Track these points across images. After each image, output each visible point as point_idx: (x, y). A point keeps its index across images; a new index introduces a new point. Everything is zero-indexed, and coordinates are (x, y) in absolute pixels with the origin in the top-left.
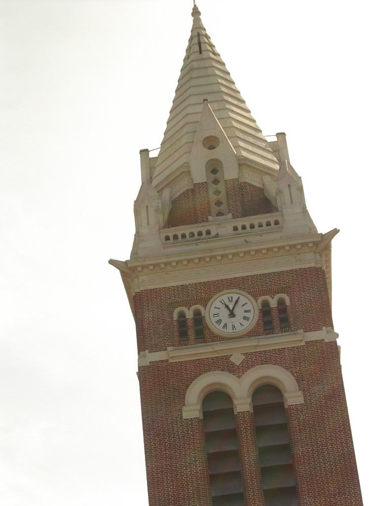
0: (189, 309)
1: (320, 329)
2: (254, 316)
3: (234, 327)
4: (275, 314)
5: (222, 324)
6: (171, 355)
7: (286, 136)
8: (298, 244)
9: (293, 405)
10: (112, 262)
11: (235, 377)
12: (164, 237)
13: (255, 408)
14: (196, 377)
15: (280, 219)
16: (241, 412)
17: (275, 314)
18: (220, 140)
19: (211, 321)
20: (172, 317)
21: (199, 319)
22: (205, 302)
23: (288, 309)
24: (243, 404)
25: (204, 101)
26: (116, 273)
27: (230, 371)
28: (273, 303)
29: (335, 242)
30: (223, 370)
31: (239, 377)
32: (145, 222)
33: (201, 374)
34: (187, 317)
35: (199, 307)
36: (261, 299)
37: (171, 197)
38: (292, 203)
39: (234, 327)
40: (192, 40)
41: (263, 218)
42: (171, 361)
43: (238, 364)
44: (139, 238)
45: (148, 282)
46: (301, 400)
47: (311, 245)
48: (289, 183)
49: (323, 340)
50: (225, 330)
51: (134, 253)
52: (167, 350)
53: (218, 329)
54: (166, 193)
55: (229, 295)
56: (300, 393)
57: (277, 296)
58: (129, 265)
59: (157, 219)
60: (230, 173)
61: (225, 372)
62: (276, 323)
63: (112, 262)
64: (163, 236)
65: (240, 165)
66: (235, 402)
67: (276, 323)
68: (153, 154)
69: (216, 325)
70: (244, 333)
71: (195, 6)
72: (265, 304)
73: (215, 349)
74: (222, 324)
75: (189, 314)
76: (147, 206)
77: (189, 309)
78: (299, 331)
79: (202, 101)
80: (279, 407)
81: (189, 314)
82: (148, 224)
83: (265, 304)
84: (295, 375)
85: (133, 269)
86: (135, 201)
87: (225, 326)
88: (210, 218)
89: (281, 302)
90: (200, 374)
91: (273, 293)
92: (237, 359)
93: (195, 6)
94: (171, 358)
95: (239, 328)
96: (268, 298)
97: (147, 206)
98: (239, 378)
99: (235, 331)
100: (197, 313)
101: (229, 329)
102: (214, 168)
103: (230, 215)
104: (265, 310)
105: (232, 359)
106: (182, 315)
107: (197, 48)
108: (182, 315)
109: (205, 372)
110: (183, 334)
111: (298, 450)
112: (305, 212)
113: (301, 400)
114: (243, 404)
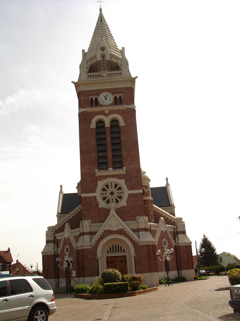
1: (131, 105)
2: (112, 100)
3: (106, 103)
4: (118, 100)
5: (103, 102)
10: (72, 82)
15: (121, 72)
17: (118, 100)
19: (100, 101)
20: (89, 99)
21: (96, 100)
23: (122, 98)
24: (107, 125)
26: (74, 85)
28: (118, 96)
29: (136, 80)
36: (114, 95)
39: (106, 103)
41: (117, 72)
42: (88, 111)
45: (82, 88)
46: (124, 125)
51: (79, 80)
53: (102, 103)
54: (89, 62)
55: (106, 93)
56: (124, 122)
57: (119, 95)
59: (86, 70)
62: (118, 102)
63: (72, 82)
67: (118, 102)
68: (86, 51)
72: (116, 97)
74: (103, 102)
75: (94, 98)
80: (118, 126)
81: (94, 98)
83: (116, 97)
85: (78, 84)
86: (80, 65)
87: (104, 102)
88: (101, 71)
89: (120, 96)
91: (118, 93)
92: (107, 112)
95: (108, 103)
96: (116, 95)
100: (96, 98)
101: (105, 103)
102: (103, 56)
103: (107, 70)
104: (115, 98)
105: (105, 112)
106: (92, 98)
107: (100, 21)
111: (122, 138)
113: (124, 125)
114: (107, 125)
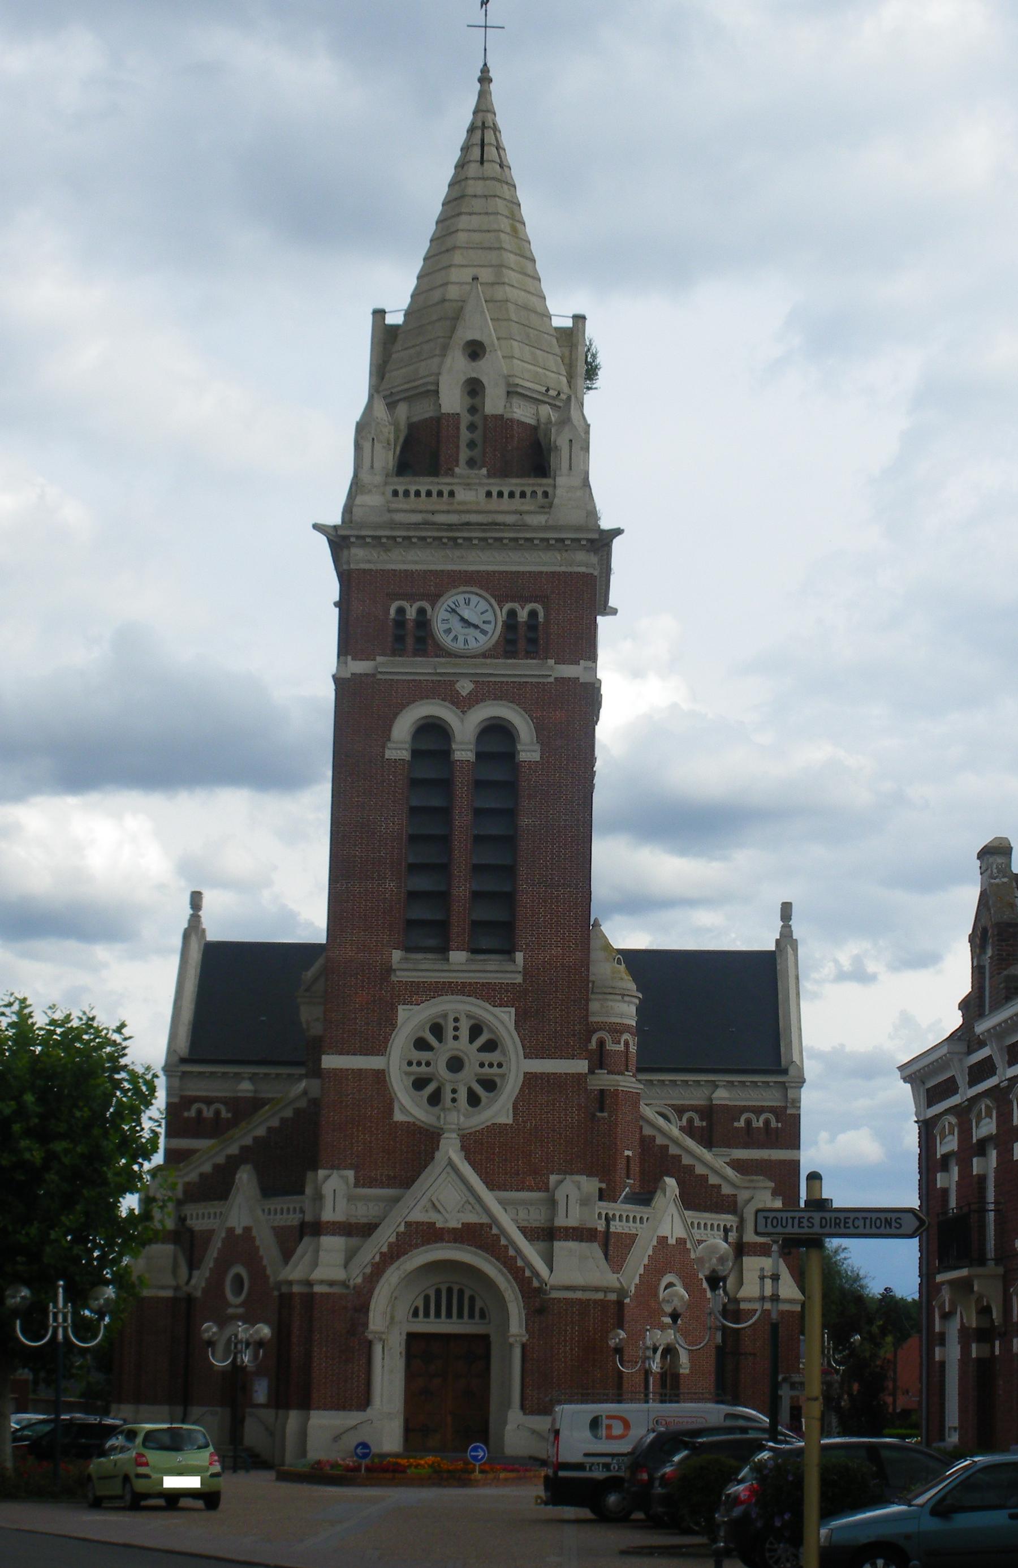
0: (411, 606)
1: (577, 663)
2: (495, 631)
3: (466, 641)
4: (522, 631)
5: (452, 636)
6: (379, 670)
7: (587, 321)
8: (568, 539)
9: (526, 761)
10: (316, 527)
11: (458, 711)
12: (391, 491)
13: (479, 755)
14: (408, 704)
15: (550, 490)
16: (459, 761)
17: (522, 631)
18: (488, 350)
19: (439, 627)
20: (387, 612)
21: (423, 622)
22: (434, 598)
23: (540, 628)
24: (464, 751)
25: (473, 279)
26: (322, 543)
27: (453, 703)
28: (523, 615)
29: (617, 543)
30: (444, 700)
31: (464, 712)
32: (367, 463)
33: (415, 701)
34: (407, 617)
35: (425, 604)
36: (508, 606)
37: (408, 418)
38: (570, 469)
39: (466, 641)
40: (472, 131)
41: (528, 484)
42: (379, 676)
43: (464, 695)
44: (356, 487)
45: (360, 557)
46: (536, 756)
47: (584, 542)
48: (571, 438)
49: (578, 678)
50: (454, 645)
51: (348, 509)
52: (375, 660)
53: (446, 640)
54: (402, 409)
55: (467, 596)
56: (537, 747)
57: (529, 607)
58: (341, 532)
59: (386, 458)
60: (494, 403)
61: (446, 703)
62: (522, 644)
63: (316, 527)
64: (389, 490)
65: (508, 393)
66: (453, 746)
67: (522, 644)
68: (396, 319)
69: (444, 636)
70: (478, 653)
71: (485, 65)
72: (512, 614)
73: (438, 671)
74: (452, 636)
75: (411, 613)
76: (373, 439)
77: (411, 606)
78: (549, 660)
79: (471, 281)
80: (509, 756)
81: (411, 613)
82: (372, 467)
83: (512, 614)
84: (535, 721)
85: (345, 538)
86: (358, 424)
87: (456, 638)
88: (457, 470)
89: (533, 614)
90: (414, 701)
91: (524, 600)
92: (465, 687)
93: (485, 65)
94: (380, 673)
95: (472, 644)
96: (516, 606)
97: (373, 439)
98: (463, 714)
99: (467, 647)
100: (422, 611)
101: (460, 644)
102: (474, 388)
103: (484, 471)
104: (511, 623)
105: (458, 686)
106: (401, 611)
107: (476, 152)
108: (401, 611)
109: (422, 698)
110: (400, 639)
111: (525, 821)
112: (586, 484)
113: (536, 756)
114: (464, 751)
